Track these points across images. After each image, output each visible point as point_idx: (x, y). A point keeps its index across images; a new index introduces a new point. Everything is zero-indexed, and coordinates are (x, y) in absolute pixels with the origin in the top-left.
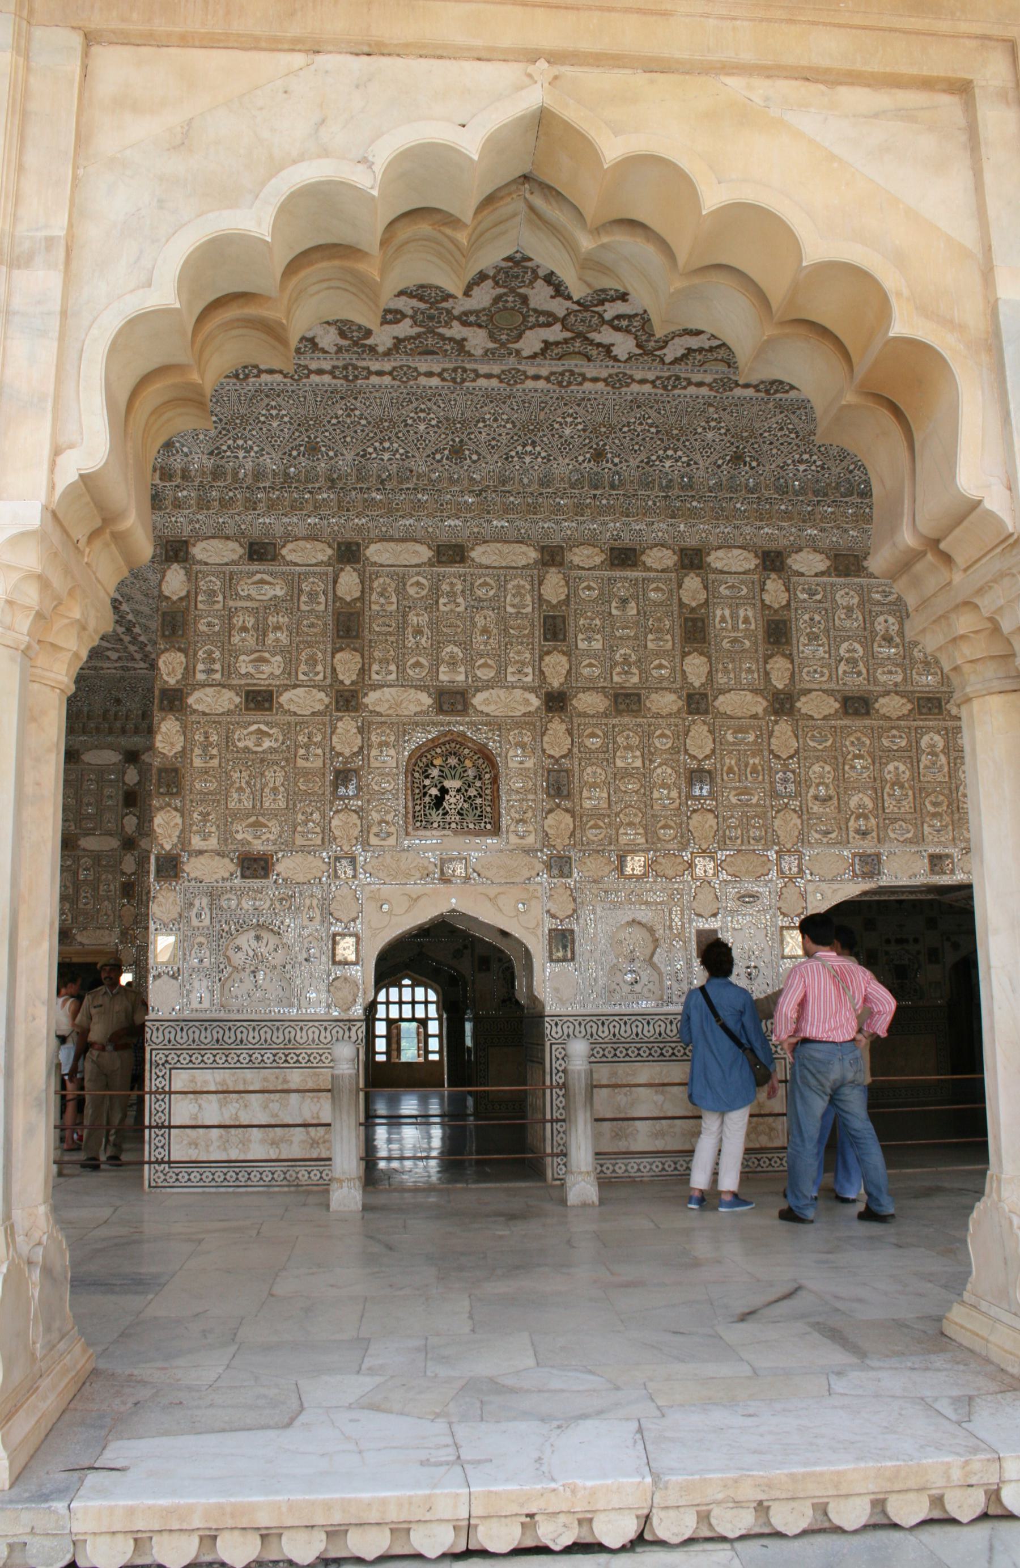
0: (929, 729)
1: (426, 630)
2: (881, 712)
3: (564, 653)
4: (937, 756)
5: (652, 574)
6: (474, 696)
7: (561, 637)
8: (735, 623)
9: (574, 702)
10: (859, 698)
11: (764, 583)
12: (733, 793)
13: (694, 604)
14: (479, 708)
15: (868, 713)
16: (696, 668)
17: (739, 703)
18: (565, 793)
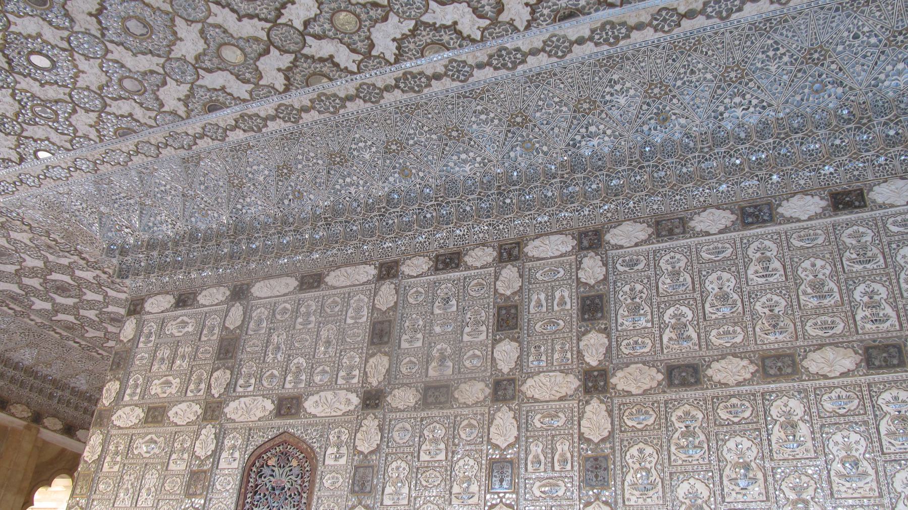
1: (283, 346)
3: (386, 354)
4: (794, 426)
5: (473, 272)
6: (306, 400)
7: (386, 339)
8: (550, 305)
9: (388, 399)
10: (688, 366)
11: (581, 263)
12: (538, 484)
13: (508, 293)
14: (309, 411)
15: (698, 382)
16: (506, 354)
17: (548, 385)
18: (368, 489)
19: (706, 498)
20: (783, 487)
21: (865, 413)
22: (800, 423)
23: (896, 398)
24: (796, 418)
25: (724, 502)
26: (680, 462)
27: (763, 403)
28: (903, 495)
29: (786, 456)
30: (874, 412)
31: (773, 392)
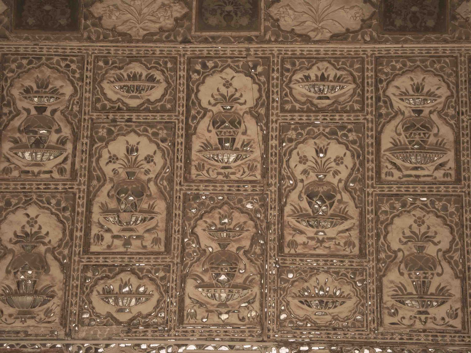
0: (223, 62)
2: (107, 22)
4: (236, 122)
15: (73, 26)
19: (55, 242)
20: (199, 230)
21: (362, 110)
22: (248, 118)
23: (418, 89)
24: (241, 109)
25: (86, 251)
26: (15, 173)
27: (189, 78)
28: (400, 254)
29: (213, 175)
30: (378, 108)
31: (209, 58)
